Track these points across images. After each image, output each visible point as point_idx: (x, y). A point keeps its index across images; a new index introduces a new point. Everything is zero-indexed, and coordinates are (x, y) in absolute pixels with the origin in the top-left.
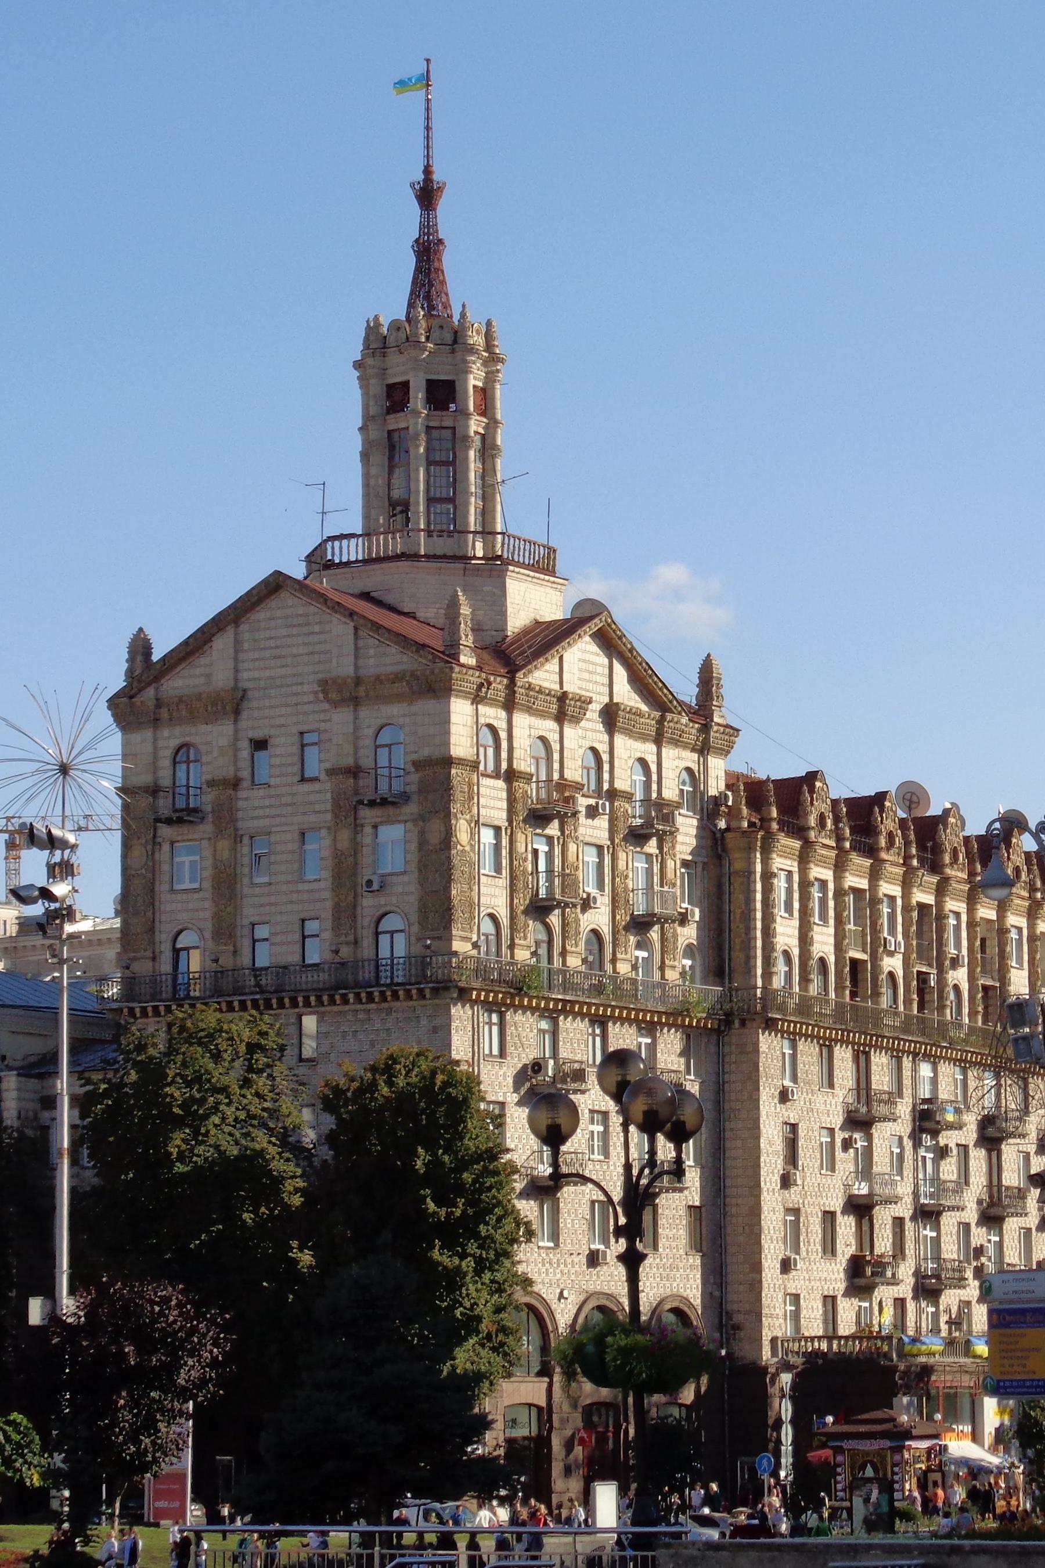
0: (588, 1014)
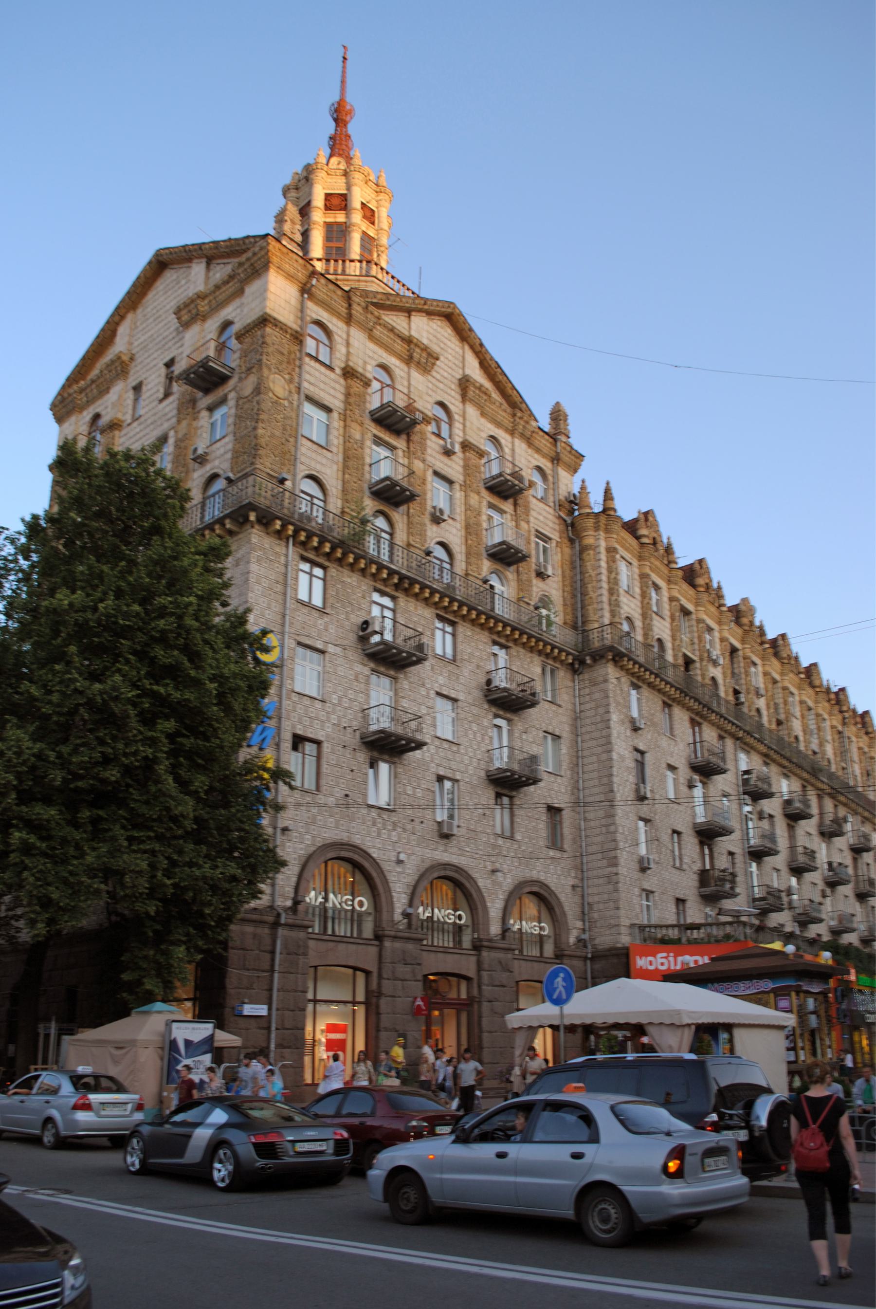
0: (436, 605)
